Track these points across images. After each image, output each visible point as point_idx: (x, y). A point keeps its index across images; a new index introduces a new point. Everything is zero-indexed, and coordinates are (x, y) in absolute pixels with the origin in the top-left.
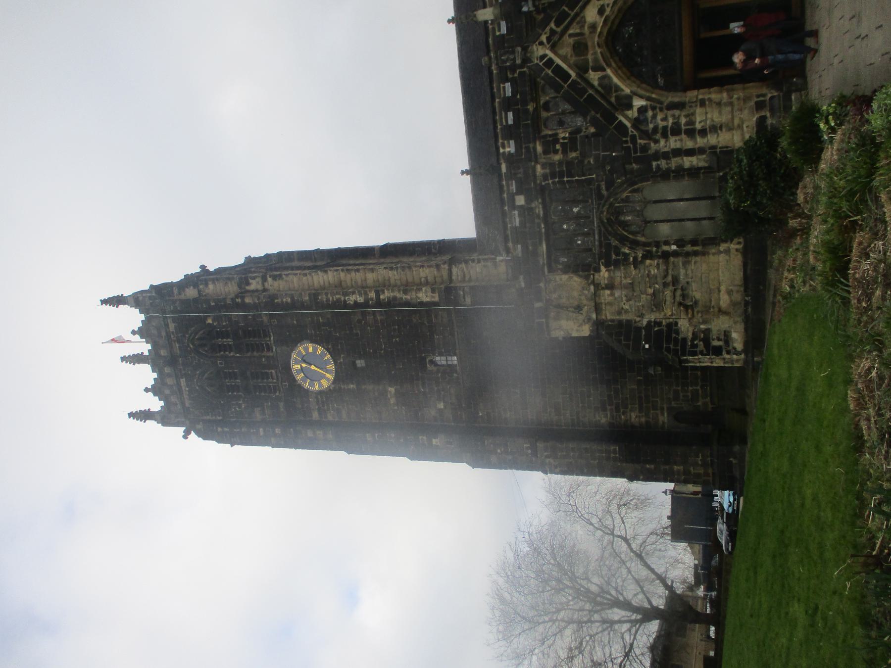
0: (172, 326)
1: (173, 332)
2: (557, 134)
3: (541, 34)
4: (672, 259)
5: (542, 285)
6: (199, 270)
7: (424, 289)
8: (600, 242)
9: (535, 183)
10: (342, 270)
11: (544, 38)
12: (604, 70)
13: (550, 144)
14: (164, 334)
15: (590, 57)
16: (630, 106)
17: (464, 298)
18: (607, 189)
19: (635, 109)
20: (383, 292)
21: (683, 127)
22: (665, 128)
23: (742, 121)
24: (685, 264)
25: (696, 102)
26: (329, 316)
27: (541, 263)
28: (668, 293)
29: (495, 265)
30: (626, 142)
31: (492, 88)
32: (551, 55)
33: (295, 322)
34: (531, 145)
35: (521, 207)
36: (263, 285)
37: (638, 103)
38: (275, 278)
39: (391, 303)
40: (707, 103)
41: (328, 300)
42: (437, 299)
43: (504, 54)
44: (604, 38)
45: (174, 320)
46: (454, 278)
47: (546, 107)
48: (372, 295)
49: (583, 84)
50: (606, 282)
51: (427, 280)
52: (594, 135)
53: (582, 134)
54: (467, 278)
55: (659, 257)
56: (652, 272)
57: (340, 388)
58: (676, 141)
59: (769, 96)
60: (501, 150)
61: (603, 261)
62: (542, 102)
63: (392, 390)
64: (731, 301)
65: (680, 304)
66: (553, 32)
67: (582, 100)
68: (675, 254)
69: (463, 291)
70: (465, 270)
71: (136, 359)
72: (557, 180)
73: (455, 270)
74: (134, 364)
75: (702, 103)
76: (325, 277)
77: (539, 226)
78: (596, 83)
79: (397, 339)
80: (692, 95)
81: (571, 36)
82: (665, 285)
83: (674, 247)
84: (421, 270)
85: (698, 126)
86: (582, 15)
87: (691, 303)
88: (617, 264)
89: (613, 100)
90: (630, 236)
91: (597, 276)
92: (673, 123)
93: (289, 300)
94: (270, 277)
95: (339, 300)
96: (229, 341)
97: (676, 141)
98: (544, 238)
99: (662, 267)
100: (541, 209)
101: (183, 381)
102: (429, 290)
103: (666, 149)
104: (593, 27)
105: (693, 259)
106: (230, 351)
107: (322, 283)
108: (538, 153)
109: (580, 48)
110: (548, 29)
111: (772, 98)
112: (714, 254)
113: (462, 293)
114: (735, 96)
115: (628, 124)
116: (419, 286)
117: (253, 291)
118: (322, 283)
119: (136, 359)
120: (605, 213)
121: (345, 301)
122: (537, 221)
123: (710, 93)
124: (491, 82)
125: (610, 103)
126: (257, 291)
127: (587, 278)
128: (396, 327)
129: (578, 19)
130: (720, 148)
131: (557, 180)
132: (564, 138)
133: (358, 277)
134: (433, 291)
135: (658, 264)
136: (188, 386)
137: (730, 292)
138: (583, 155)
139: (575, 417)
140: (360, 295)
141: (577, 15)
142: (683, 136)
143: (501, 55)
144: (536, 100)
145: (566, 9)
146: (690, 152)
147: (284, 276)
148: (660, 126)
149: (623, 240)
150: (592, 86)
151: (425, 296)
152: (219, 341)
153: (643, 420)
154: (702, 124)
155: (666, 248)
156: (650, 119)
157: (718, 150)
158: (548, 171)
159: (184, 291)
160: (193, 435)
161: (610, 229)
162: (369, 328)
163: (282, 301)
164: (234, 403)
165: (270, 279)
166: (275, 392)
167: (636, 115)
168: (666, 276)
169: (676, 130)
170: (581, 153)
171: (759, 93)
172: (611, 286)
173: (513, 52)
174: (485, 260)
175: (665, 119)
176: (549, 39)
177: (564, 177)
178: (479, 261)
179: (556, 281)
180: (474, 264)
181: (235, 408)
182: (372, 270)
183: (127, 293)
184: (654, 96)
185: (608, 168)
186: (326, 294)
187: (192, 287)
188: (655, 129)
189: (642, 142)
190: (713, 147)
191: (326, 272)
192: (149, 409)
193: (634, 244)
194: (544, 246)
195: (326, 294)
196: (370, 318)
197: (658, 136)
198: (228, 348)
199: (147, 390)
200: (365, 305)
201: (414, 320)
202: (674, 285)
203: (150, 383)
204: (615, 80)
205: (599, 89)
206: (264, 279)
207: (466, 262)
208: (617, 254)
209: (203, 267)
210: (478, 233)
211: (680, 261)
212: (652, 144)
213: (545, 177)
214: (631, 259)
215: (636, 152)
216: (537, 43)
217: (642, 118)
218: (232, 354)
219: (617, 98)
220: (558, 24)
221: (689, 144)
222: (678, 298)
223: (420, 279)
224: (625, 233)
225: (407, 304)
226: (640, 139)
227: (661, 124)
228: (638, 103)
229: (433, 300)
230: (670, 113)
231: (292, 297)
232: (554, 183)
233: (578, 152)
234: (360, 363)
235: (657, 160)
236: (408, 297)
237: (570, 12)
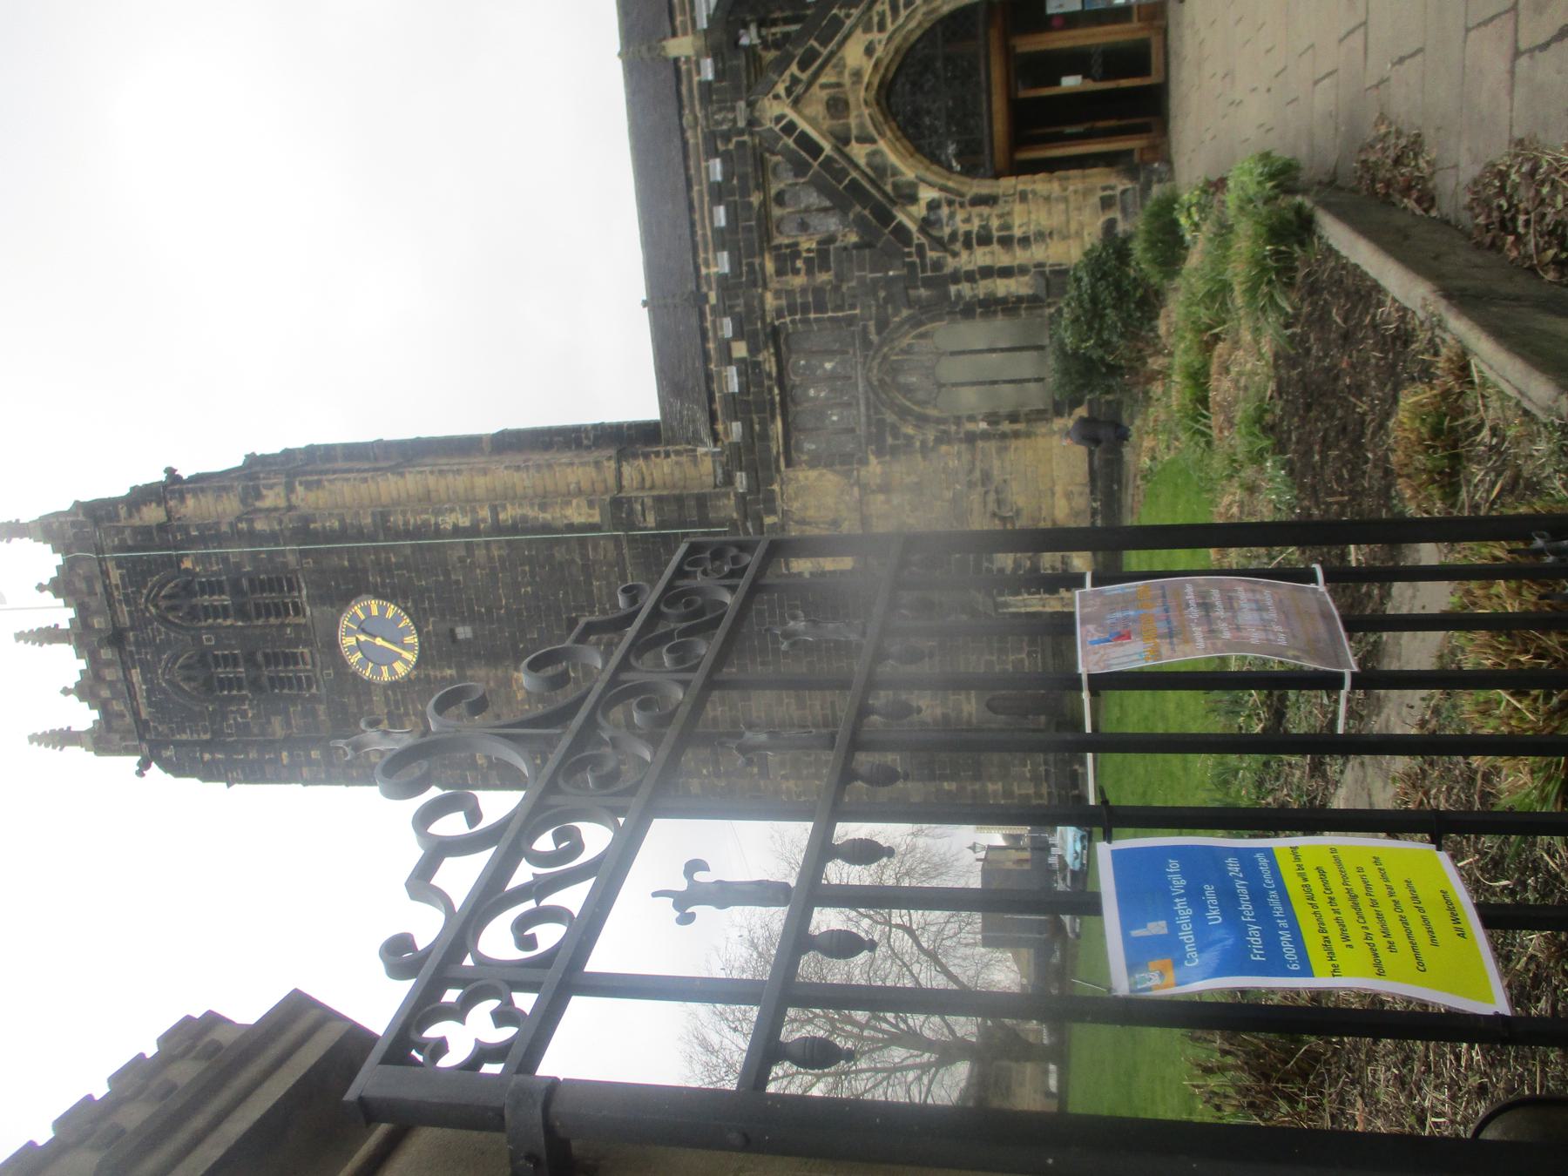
0: (115, 576)
1: (117, 586)
2: (796, 244)
3: (776, 83)
4: (980, 444)
5: (776, 487)
6: (162, 477)
7: (575, 502)
8: (868, 417)
10: (432, 472)
11: (781, 89)
12: (873, 141)
13: (787, 259)
14: (99, 588)
15: (853, 122)
16: (913, 199)
17: (644, 515)
18: (879, 332)
19: (923, 203)
20: (504, 508)
21: (996, 234)
22: (968, 234)
23: (1082, 226)
24: (1002, 450)
25: (1014, 194)
26: (408, 552)
27: (775, 451)
28: (975, 497)
29: (695, 460)
30: (909, 255)
31: (687, 168)
32: (792, 115)
33: (346, 563)
34: (757, 261)
35: (742, 361)
36: (288, 500)
37: (927, 194)
38: (308, 486)
39: (514, 528)
40: (1030, 196)
41: (406, 523)
42: (597, 519)
43: (720, 110)
44: (874, 92)
45: (120, 564)
46: (625, 483)
47: (780, 199)
48: (485, 513)
49: (843, 163)
50: (878, 481)
51: (580, 489)
52: (856, 246)
53: (838, 244)
54: (648, 484)
55: (960, 441)
56: (950, 464)
57: (427, 676)
58: (984, 254)
59: (1120, 188)
60: (704, 271)
61: (873, 447)
62: (773, 192)
64: (1072, 508)
65: (994, 515)
66: (795, 81)
67: (841, 187)
68: (985, 436)
69: (643, 504)
70: (644, 469)
71: (50, 635)
72: (798, 317)
74: (41, 645)
75: (1023, 197)
76: (401, 482)
77: (770, 390)
78: (862, 162)
79: (529, 589)
80: (1007, 184)
81: (823, 86)
82: (971, 485)
83: (983, 425)
84: (569, 470)
85: (1017, 232)
86: (839, 55)
87: (1010, 514)
88: (894, 451)
89: (889, 188)
90: (916, 408)
91: (863, 473)
92: (982, 227)
93: (336, 524)
94: (301, 484)
95: (426, 524)
96: (226, 600)
97: (984, 254)
98: (778, 411)
99: (966, 457)
101: (136, 675)
102: (584, 503)
103: (970, 267)
104: (857, 74)
105: (1014, 443)
106: (226, 617)
107: (394, 494)
108: (768, 274)
109: (837, 106)
110: (787, 74)
111: (1124, 192)
112: (1044, 436)
113: (639, 508)
114: (1071, 188)
115: (912, 227)
116: (567, 497)
117: (269, 510)
118: (394, 494)
119: (50, 635)
120: (875, 371)
121: (437, 524)
122: (767, 383)
123: (1034, 182)
124: (686, 157)
125: (885, 194)
126: (276, 509)
127: (848, 474)
128: (527, 568)
129: (834, 61)
130: (1051, 265)
132: (809, 250)
133: (460, 483)
134: (591, 504)
135: (959, 453)
136: (145, 681)
137: (1069, 496)
138: (840, 278)
139: (829, 712)
140: (464, 513)
141: (832, 54)
142: (996, 247)
143: (714, 114)
144: (762, 186)
145: (816, 45)
146: (1006, 272)
147: (326, 483)
148: (961, 231)
149: (904, 413)
150: (856, 167)
151: (578, 513)
152: (206, 600)
153: (939, 711)
154: (1024, 229)
155: (970, 426)
156: (945, 220)
157: (1047, 269)
158: (784, 302)
159: (138, 510)
161: (884, 396)
162: (478, 571)
163: (324, 527)
164: (234, 708)
165: (300, 489)
166: (309, 687)
167: (924, 212)
168: (971, 471)
169: (985, 239)
170: (837, 275)
171: (1105, 184)
172: (885, 488)
173: (733, 109)
174: (678, 453)
175: (967, 220)
176: (789, 91)
178: (667, 455)
179: (797, 480)
180: (658, 460)
181: (235, 719)
182: (485, 472)
183: (28, 515)
184: (951, 184)
185: (882, 294)
186: (404, 513)
187: (154, 505)
188: (953, 236)
189: (932, 255)
190: (1040, 265)
191: (402, 475)
192: (69, 728)
193: (923, 420)
195: (404, 513)
196: (480, 553)
197: (958, 246)
198: (224, 612)
199: (66, 691)
200: (474, 530)
201: (557, 555)
202: (983, 485)
203: (72, 679)
204: (893, 159)
205: (868, 170)
206: (290, 489)
207: (646, 456)
208: (896, 436)
209: (170, 472)
210: (663, 409)
211: (992, 446)
212: (950, 259)
213: (779, 313)
214: (918, 444)
216: (770, 96)
217: (933, 217)
218: (229, 622)
219: (895, 186)
220: (803, 66)
221: (1003, 259)
222: (992, 506)
223: (568, 485)
224: (908, 404)
225: (546, 528)
227: (963, 228)
228: (927, 194)
229: (591, 520)
231: (342, 520)
232: (793, 322)
233: (832, 273)
234: (464, 632)
236: (548, 516)
237: (821, 49)
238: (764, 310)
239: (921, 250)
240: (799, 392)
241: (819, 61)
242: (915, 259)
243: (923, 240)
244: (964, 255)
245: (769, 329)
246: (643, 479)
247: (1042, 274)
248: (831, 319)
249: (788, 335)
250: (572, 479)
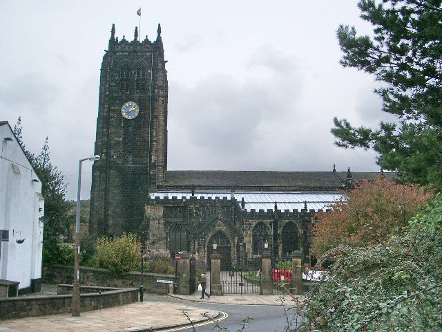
63: (121, 139)
71: (136, 34)
80: (206, 248)
88: (165, 225)
119: (136, 34)
160: (105, 53)
169: (199, 245)
172: (159, 223)
193: (170, 230)
196: (146, 135)
200: (151, 134)
221: (196, 247)
225: (151, 151)
234: (131, 129)
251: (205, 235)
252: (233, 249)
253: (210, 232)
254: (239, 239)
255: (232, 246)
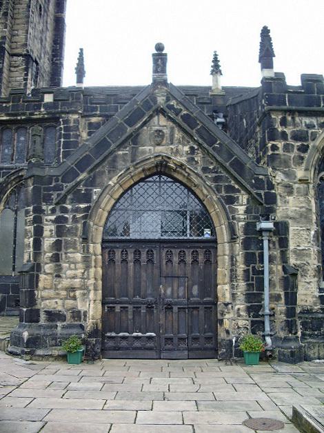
9: (63, 113)
15: (147, 148)
21: (64, 238)
30: (57, 180)
51: (14, 36)
54: (12, 69)
58: (51, 231)
66: (177, 112)
72: (63, 132)
73: (21, 58)
77: (24, 114)
81: (172, 129)
98: (12, 118)
100: (38, 117)
111: (82, 327)
131: (63, 132)
142: (53, 240)
146: (37, 244)
157: (35, 273)
158: (72, 125)
161: (12, 178)
169: (60, 231)
176: (171, 107)
177: (64, 139)
180: (23, 75)
188: (65, 210)
194: (5, 118)
197: (58, 213)
207: (26, 69)
212: (50, 207)
213: (66, 122)
215: (45, 189)
221: (47, 242)
226: (58, 195)
230: (80, 226)
232: (61, 129)
235: (35, 211)
238: (68, 113)
239: (58, 188)
240: (23, 131)
241: (188, 129)
242: (54, 184)
243: (65, 190)
244: (53, 218)
245: (58, 115)
246: (15, 67)
247: (32, 269)
248: (60, 150)
249: (56, 127)
250: (20, 32)
251: (91, 182)
252: (224, 249)
253: (113, 169)
254: (253, 199)
255: (223, 234)
